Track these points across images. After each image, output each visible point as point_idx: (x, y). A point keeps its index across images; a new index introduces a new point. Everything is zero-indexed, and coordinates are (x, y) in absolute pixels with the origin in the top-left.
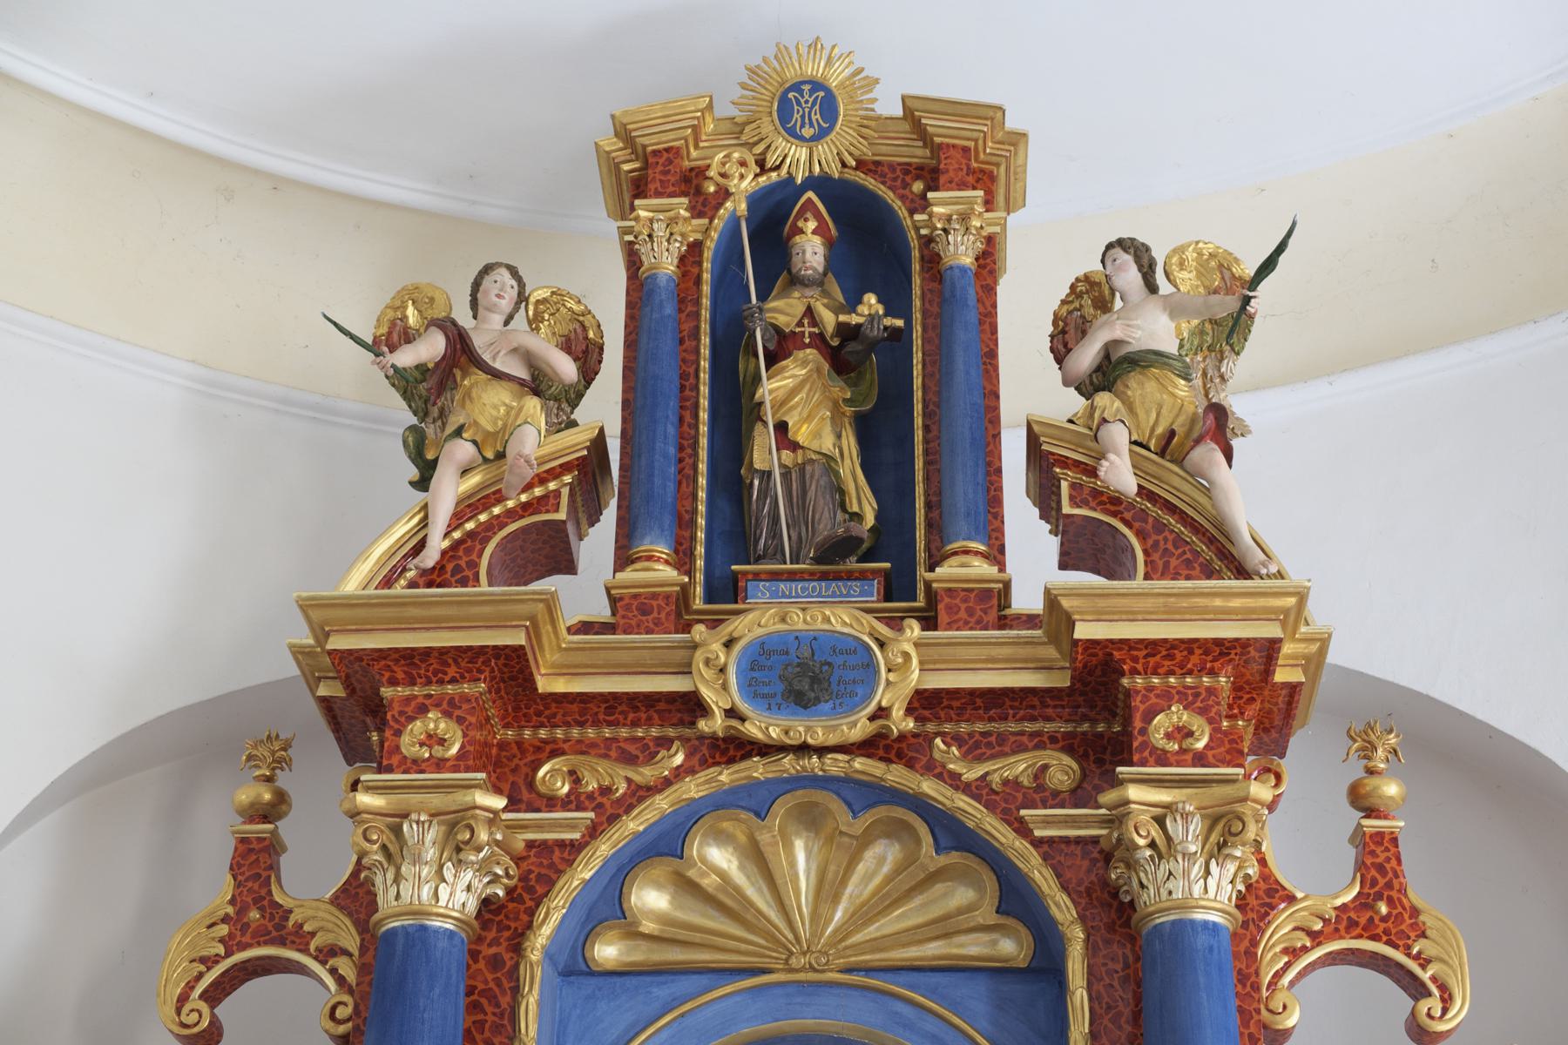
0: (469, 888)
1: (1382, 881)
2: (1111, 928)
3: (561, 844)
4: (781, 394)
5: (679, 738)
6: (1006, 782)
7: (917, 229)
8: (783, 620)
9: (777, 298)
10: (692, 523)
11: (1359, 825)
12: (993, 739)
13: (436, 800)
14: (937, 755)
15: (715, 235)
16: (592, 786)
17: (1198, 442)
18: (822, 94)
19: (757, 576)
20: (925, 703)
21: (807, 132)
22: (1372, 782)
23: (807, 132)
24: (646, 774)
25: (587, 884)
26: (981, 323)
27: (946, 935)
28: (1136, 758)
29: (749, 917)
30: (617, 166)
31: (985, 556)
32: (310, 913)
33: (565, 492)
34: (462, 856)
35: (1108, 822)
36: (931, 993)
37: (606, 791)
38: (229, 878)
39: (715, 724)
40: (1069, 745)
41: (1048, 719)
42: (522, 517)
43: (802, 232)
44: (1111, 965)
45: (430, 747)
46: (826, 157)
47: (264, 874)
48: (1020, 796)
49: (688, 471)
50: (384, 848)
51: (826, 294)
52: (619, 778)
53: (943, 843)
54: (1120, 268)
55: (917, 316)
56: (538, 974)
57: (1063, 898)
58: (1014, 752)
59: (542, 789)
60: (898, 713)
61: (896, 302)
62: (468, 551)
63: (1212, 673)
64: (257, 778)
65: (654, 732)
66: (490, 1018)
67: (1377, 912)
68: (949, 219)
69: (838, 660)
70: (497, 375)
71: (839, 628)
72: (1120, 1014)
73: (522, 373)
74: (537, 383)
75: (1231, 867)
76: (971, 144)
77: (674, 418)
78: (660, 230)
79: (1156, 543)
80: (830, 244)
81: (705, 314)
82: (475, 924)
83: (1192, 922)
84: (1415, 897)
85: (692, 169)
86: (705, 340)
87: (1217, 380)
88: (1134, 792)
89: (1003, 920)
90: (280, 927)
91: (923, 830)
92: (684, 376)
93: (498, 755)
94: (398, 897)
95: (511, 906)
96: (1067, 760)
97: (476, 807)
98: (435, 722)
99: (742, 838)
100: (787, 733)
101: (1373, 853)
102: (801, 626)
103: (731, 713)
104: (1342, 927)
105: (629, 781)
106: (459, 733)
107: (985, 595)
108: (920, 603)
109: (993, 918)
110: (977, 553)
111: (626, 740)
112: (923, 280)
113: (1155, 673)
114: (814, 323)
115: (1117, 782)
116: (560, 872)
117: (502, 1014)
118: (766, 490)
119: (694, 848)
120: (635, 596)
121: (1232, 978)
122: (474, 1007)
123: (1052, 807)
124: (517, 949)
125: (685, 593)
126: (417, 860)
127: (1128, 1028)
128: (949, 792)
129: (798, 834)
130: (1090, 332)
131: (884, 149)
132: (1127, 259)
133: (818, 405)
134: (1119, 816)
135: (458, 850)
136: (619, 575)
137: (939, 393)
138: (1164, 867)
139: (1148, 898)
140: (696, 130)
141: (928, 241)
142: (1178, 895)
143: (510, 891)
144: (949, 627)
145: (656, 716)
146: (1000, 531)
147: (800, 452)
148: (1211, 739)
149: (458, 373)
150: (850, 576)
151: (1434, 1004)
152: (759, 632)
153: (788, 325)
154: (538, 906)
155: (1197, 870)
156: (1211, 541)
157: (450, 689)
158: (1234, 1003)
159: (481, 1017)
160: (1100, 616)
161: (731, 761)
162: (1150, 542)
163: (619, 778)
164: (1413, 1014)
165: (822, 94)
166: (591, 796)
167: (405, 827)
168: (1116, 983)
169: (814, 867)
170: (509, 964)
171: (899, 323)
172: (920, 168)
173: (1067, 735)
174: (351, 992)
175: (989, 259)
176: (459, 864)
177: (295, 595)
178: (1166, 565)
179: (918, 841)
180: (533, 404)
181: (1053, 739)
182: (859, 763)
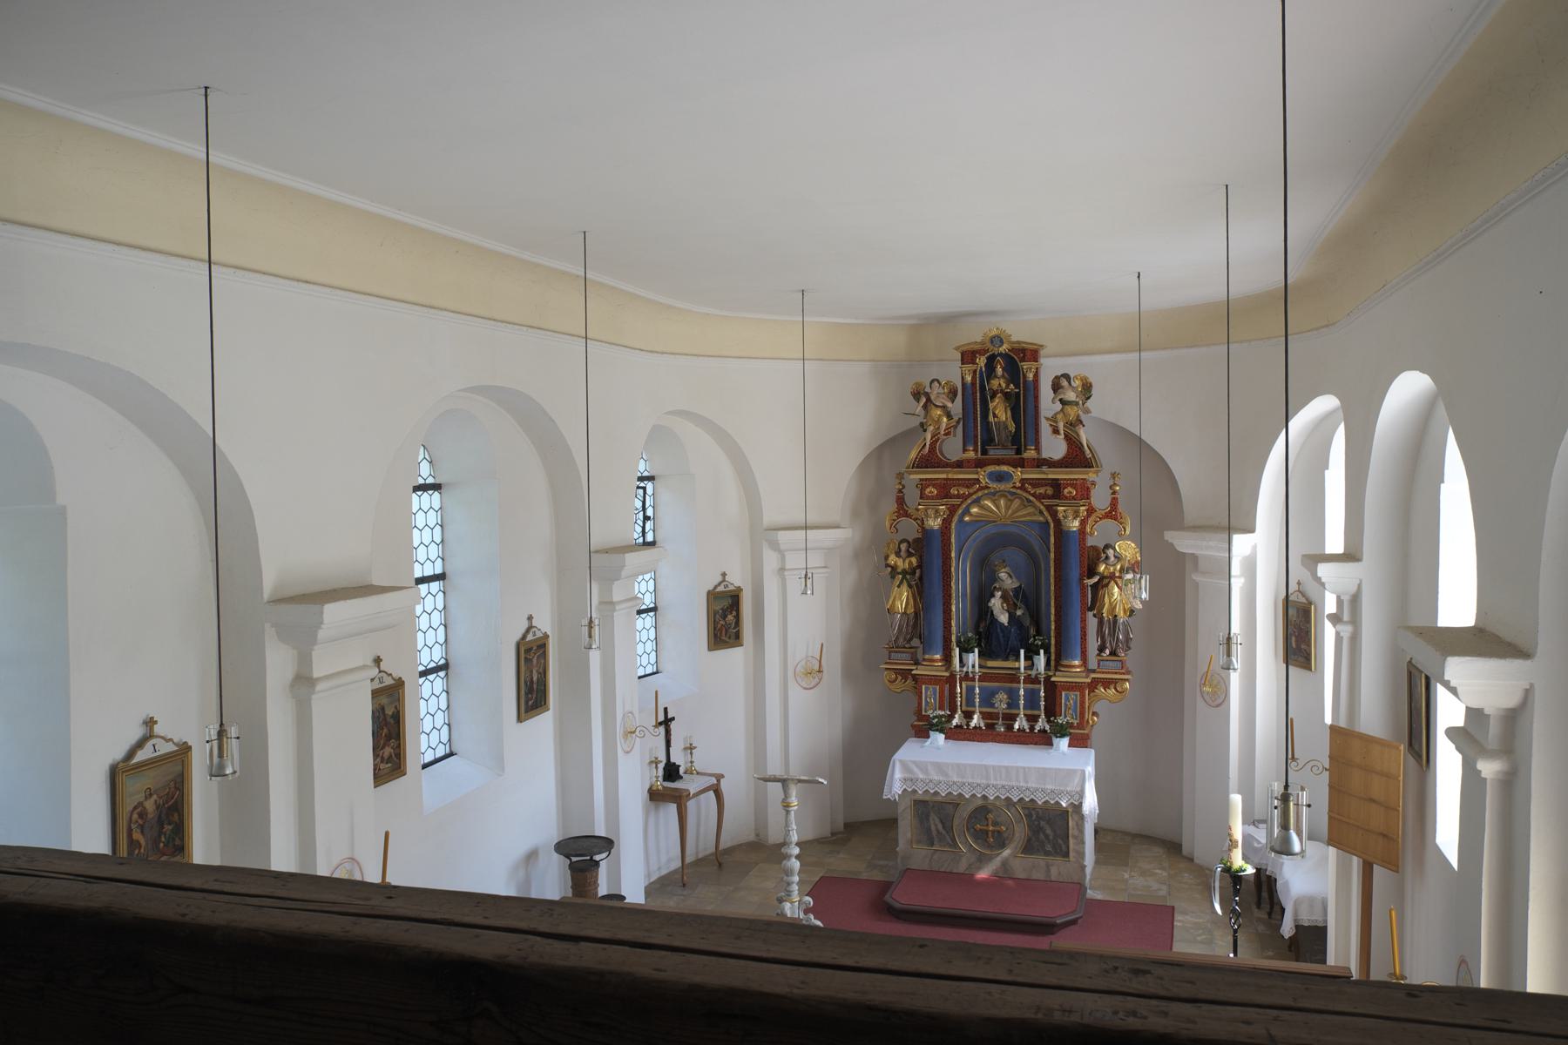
24: (971, 491)
37: (964, 494)
46: (1004, 348)
61: (1017, 386)
70: (937, 406)
175: (1036, 375)
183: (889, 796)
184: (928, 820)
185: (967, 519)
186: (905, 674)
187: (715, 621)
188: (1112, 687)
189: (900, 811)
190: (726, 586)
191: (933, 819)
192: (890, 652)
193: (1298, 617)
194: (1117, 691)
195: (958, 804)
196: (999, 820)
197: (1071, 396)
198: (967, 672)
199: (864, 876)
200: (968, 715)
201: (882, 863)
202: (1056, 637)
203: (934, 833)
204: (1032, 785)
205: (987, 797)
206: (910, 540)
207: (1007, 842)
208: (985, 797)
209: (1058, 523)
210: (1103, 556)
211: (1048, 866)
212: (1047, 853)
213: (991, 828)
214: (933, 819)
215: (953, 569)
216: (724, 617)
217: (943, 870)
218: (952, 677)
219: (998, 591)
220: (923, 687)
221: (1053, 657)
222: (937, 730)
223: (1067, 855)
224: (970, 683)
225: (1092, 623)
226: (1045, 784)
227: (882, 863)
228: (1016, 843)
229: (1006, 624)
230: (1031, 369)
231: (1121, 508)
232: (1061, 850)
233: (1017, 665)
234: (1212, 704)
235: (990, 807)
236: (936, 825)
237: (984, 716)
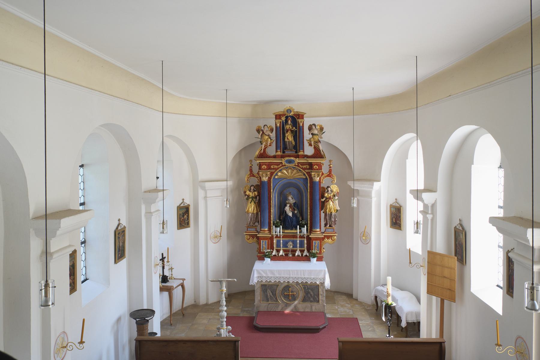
24: (279, 167)
37: (276, 168)
61: (296, 128)
70: (266, 135)
96: (308, 166)
118: (286, 142)
119: (282, 171)
175: (303, 124)
183: (252, 284)
184: (266, 292)
185: (276, 177)
186: (253, 236)
187: (180, 218)
188: (330, 238)
190: (184, 204)
191: (269, 292)
192: (247, 228)
193: (396, 211)
194: (332, 240)
195: (278, 285)
196: (293, 290)
197: (316, 132)
199: (241, 315)
200: (278, 251)
201: (246, 309)
202: (310, 221)
203: (269, 297)
204: (306, 276)
206: (255, 185)
207: (296, 298)
208: (288, 282)
209: (311, 178)
210: (326, 190)
211: (311, 306)
212: (311, 302)
213: (291, 293)
214: (269, 292)
215: (272, 196)
216: (183, 216)
217: (272, 310)
220: (261, 241)
221: (309, 228)
222: (268, 257)
223: (318, 302)
225: (323, 215)
227: (246, 309)
229: (291, 216)
230: (301, 122)
232: (316, 300)
233: (296, 231)
234: (364, 242)
237: (284, 251)
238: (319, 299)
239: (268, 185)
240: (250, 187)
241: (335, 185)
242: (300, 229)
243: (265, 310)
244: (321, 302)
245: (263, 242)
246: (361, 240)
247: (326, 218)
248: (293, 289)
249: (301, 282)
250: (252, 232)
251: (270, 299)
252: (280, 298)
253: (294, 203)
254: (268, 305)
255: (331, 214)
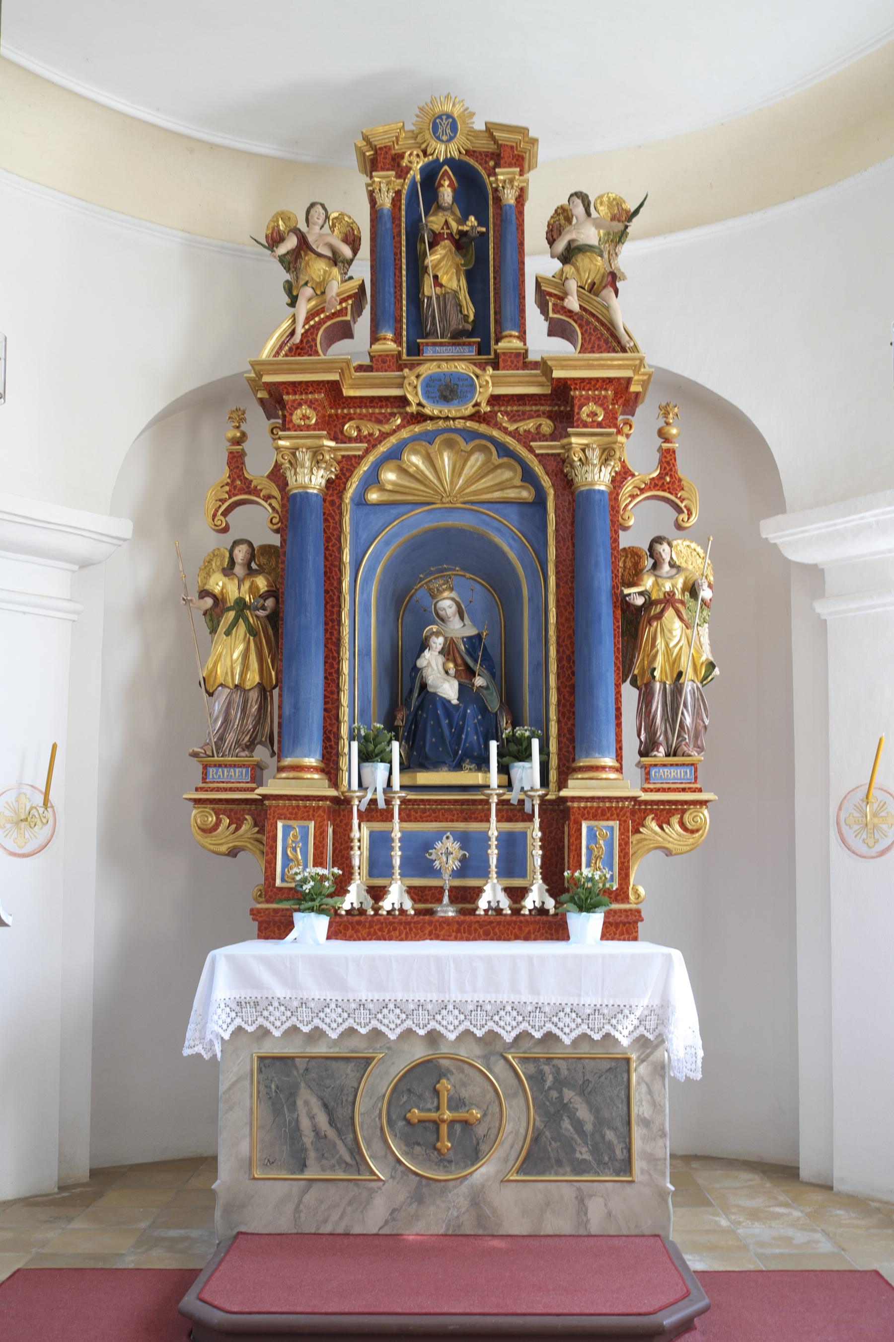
0: (322, 477)
1: (668, 468)
2: (564, 488)
3: (355, 456)
4: (435, 262)
5: (399, 413)
6: (525, 431)
7: (491, 184)
8: (439, 367)
9: (433, 215)
10: (401, 321)
11: (661, 446)
12: (520, 413)
13: (308, 442)
14: (498, 420)
15: (406, 187)
16: (366, 433)
17: (604, 287)
18: (451, 120)
19: (427, 344)
20: (494, 400)
21: (445, 138)
22: (668, 428)
23: (445, 138)
24: (386, 428)
25: (365, 472)
26: (518, 229)
27: (502, 490)
28: (575, 424)
29: (427, 483)
30: (364, 154)
31: (518, 337)
32: (259, 482)
33: (349, 307)
34: (320, 465)
35: (563, 447)
36: (496, 512)
37: (371, 435)
38: (227, 468)
39: (413, 409)
40: (550, 416)
41: (542, 405)
42: (332, 318)
43: (443, 186)
44: (564, 504)
45: (304, 420)
47: (240, 466)
48: (530, 437)
49: (399, 297)
50: (290, 462)
51: (453, 213)
52: (376, 430)
53: (501, 454)
54: (575, 206)
55: (491, 226)
56: (349, 507)
57: (546, 478)
58: (529, 418)
59: (346, 434)
60: (483, 404)
61: (482, 220)
62: (312, 334)
63: (606, 389)
64: (233, 427)
65: (389, 410)
66: (332, 524)
67: (666, 480)
68: (505, 181)
69: (461, 383)
70: (319, 255)
71: (461, 370)
72: (567, 522)
73: (329, 253)
74: (336, 259)
75: (609, 468)
76: (515, 145)
77: (392, 275)
78: (384, 188)
79: (586, 330)
80: (454, 191)
81: (403, 225)
82: (325, 490)
83: (594, 490)
84: (681, 473)
85: (395, 154)
86: (404, 237)
87: (614, 255)
88: (574, 440)
89: (523, 484)
90: (248, 488)
91: (493, 449)
92: (395, 254)
93: (329, 420)
94: (296, 480)
95: (337, 481)
96: (549, 422)
97: (323, 446)
98: (305, 410)
99: (424, 452)
100: (441, 412)
101: (666, 457)
102: (446, 370)
103: (419, 404)
104: (652, 487)
105: (380, 431)
106: (315, 414)
107: (518, 355)
108: (492, 356)
109: (519, 483)
110: (514, 337)
111: (378, 414)
112: (494, 208)
113: (584, 389)
114: (448, 228)
115: (568, 435)
116: (355, 468)
117: (336, 523)
118: (430, 304)
119: (405, 457)
120: (380, 356)
121: (608, 509)
122: (326, 520)
123: (543, 441)
124: (341, 498)
125: (400, 354)
126: (303, 466)
127: (569, 528)
128: (503, 435)
129: (445, 450)
130: (563, 233)
131: (477, 145)
132: (578, 202)
133: (450, 267)
134: (568, 447)
135: (318, 462)
136: (373, 347)
137: (500, 262)
138: (585, 468)
139: (578, 480)
140: (397, 138)
141: (496, 190)
142: (589, 479)
143: (336, 476)
144: (504, 369)
145: (389, 404)
146: (524, 324)
147: (443, 288)
148: (604, 416)
149: (303, 253)
150: (464, 344)
151: (685, 516)
152: (429, 372)
153: (437, 229)
154: (347, 480)
155: (596, 470)
156: (608, 329)
157: (310, 396)
158: (608, 517)
159: (328, 524)
160: (563, 367)
161: (419, 422)
162: (584, 329)
163: (376, 430)
164: (677, 520)
165: (451, 120)
166: (365, 437)
167: (297, 454)
168: (565, 511)
169: (451, 463)
170: (337, 504)
171: (484, 229)
172: (493, 154)
173: (549, 411)
174: (277, 512)
176: (318, 468)
177: (249, 359)
178: (590, 339)
179: (491, 453)
180: (335, 271)
181: (544, 413)
182: (469, 424)
183: (199, 1049)
184: (293, 1106)
185: (373, 496)
188: (675, 820)
189: (223, 1088)
192: (205, 767)
194: (685, 829)
195: (368, 1061)
196: (465, 1093)
197: (589, 234)
198: (373, 802)
200: (377, 893)
202: (559, 721)
203: (308, 1138)
204: (550, 997)
205: (440, 1035)
206: (256, 545)
207: (483, 1147)
208: (433, 1037)
210: (649, 563)
211: (581, 1200)
212: (580, 1168)
213: (447, 1115)
214: (306, 1103)
217: (327, 1229)
218: (341, 804)
219: (437, 637)
220: (280, 825)
221: (554, 762)
222: (312, 910)
223: (626, 1166)
224: (378, 826)
225: (630, 695)
226: (579, 996)
228: (507, 1145)
229: (455, 702)
231: (683, 468)
232: (613, 1158)
233: (478, 778)
234: (864, 850)
235: (445, 1063)
236: (312, 1117)
237: (414, 893)
238: (629, 1149)
239: (328, 527)
240: (231, 552)
241: (693, 545)
242: (504, 769)
243: (284, 1225)
244: (643, 1171)
245: (286, 830)
246: (844, 841)
247: (648, 712)
248: (464, 1085)
249: (514, 1034)
250: (231, 790)
251: (312, 1155)
252: (378, 1145)
253: (470, 638)
254: (305, 1191)
255: (677, 689)
